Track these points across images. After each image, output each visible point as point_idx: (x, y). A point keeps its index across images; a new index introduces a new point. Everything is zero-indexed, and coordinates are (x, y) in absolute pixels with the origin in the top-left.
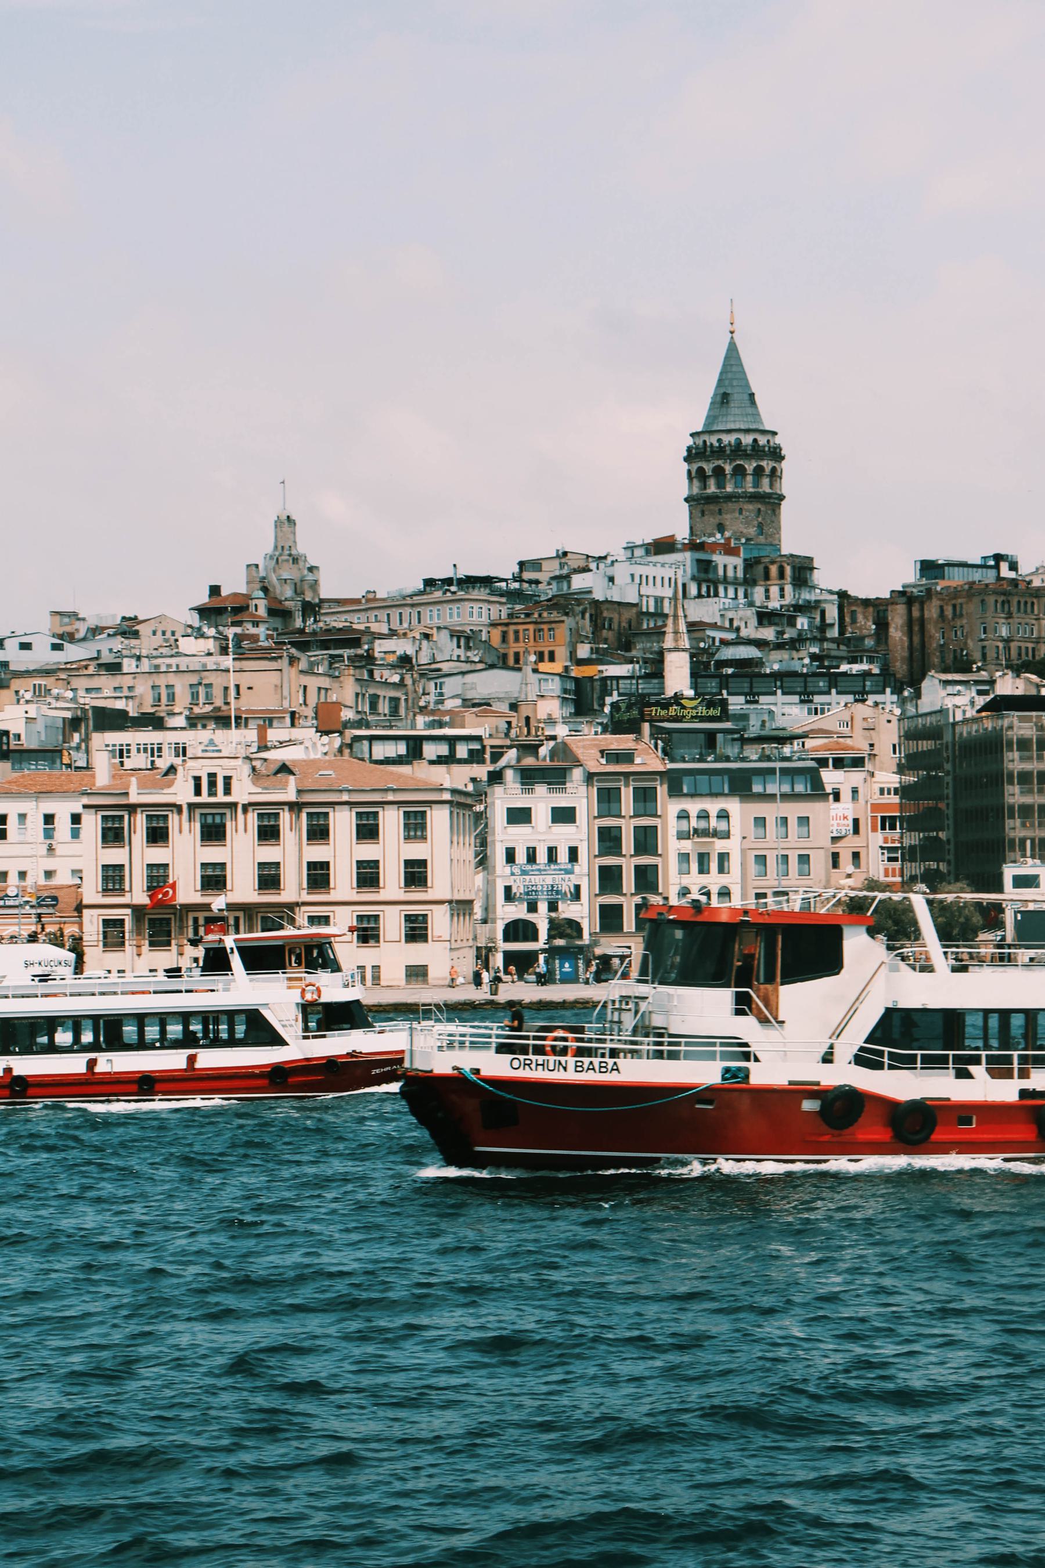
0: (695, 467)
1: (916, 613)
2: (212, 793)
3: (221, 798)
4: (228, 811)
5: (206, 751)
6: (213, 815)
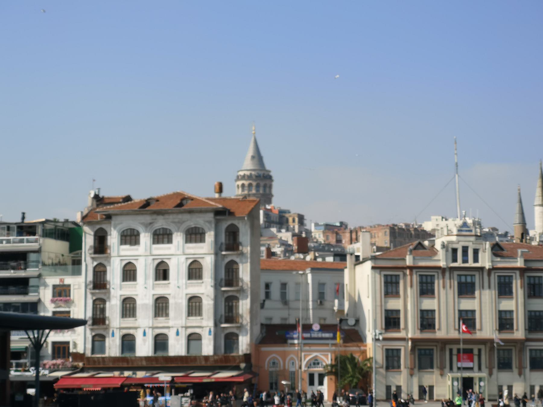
0: (240, 183)
2: (465, 261)
3: (471, 264)
4: (477, 274)
5: (461, 231)
6: (466, 276)
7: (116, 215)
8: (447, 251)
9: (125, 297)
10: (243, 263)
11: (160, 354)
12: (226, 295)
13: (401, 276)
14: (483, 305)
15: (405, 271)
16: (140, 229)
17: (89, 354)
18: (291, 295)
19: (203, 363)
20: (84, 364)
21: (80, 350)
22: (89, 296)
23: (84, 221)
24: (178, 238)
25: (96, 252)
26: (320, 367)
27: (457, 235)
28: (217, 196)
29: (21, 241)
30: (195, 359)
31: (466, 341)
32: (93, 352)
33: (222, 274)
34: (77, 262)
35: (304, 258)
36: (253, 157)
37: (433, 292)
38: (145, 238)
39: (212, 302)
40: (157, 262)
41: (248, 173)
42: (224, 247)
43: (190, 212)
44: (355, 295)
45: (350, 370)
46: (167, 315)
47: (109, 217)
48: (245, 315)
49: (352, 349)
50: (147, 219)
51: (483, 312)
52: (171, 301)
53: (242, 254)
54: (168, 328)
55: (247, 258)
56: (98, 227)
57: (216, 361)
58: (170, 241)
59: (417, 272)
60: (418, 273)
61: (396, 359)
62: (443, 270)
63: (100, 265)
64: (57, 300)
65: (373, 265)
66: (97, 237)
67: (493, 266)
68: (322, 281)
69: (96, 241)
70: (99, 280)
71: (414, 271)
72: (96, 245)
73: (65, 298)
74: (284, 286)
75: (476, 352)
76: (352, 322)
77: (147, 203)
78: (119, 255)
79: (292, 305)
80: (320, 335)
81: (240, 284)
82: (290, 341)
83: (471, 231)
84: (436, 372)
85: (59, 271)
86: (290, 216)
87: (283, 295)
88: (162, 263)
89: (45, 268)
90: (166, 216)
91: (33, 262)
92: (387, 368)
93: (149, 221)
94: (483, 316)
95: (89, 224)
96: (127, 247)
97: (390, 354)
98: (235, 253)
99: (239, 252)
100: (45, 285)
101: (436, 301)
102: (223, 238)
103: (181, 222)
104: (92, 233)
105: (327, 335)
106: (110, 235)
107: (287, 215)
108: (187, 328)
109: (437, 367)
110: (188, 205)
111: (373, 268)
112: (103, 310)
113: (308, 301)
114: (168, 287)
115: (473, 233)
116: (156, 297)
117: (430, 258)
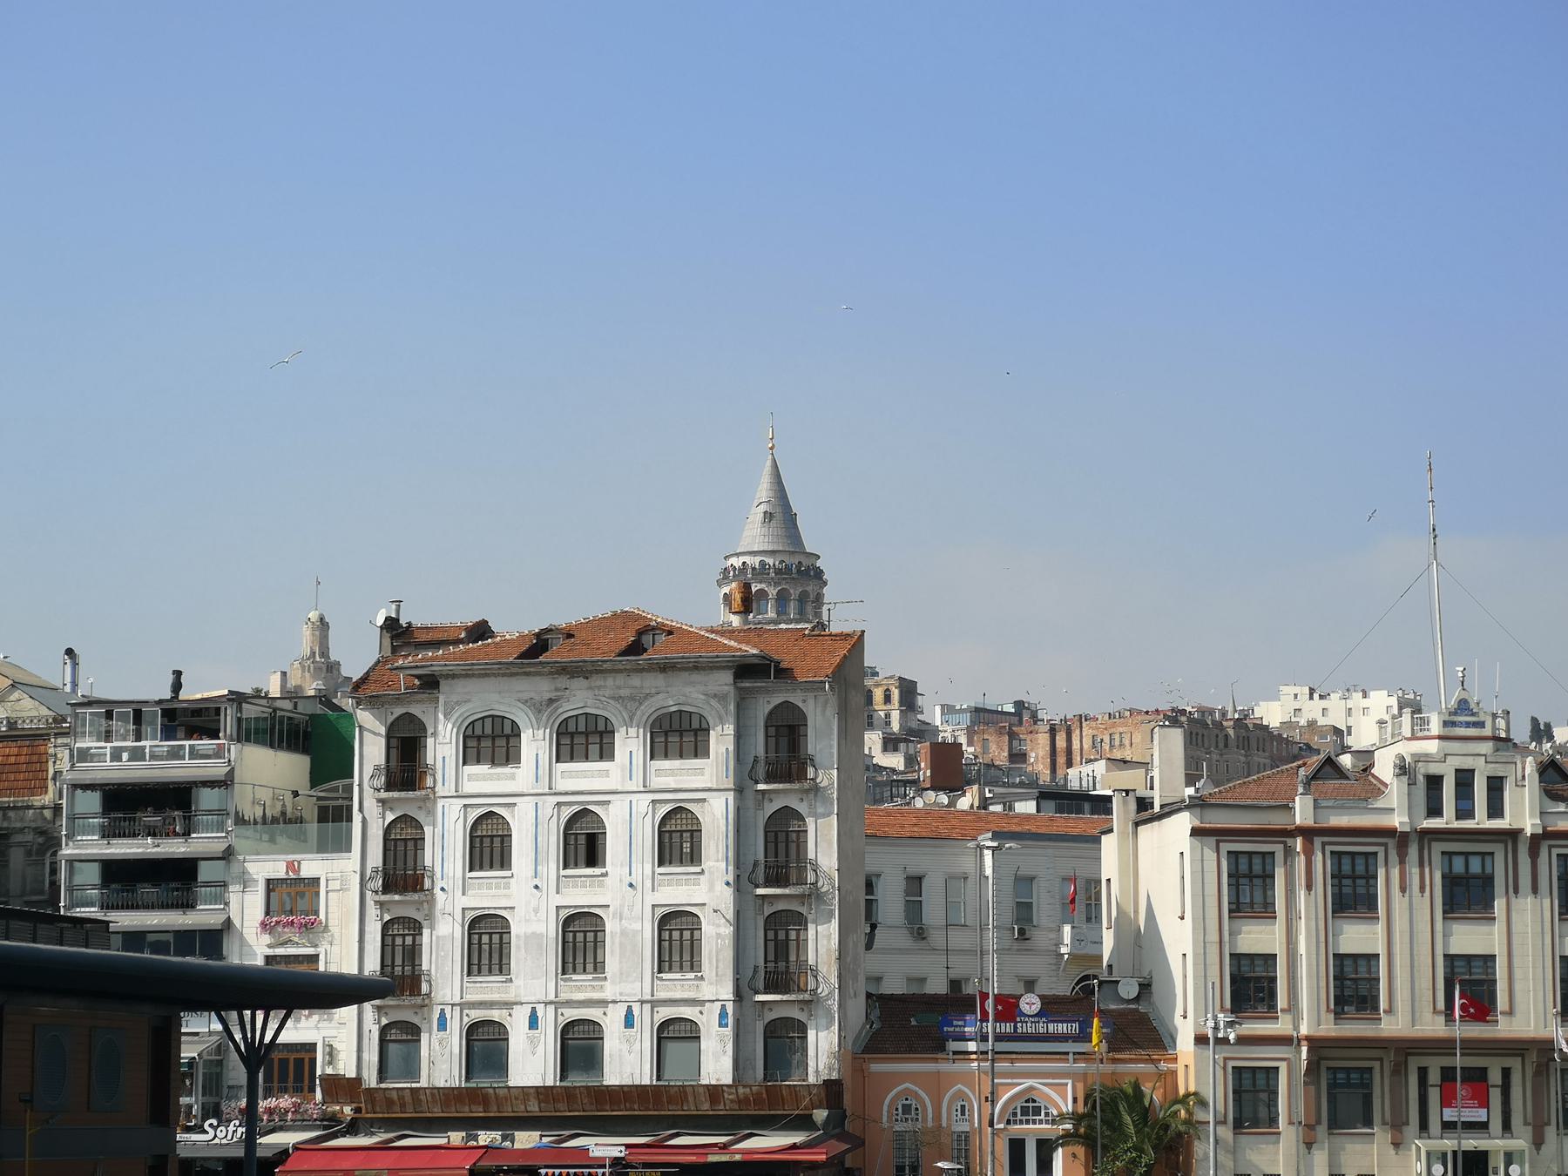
1: (1061, 742)
2: (1464, 812)
3: (1481, 820)
4: (1498, 851)
5: (1454, 724)
6: (1467, 854)
7: (454, 676)
8: (1412, 783)
9: (479, 913)
10: (816, 816)
11: (578, 1080)
12: (768, 910)
13: (1279, 857)
14: (1516, 940)
15: (1289, 841)
16: (521, 717)
17: (371, 1079)
18: (933, 913)
19: (705, 1108)
20: (358, 1110)
21: (346, 1067)
22: (372, 911)
23: (360, 694)
24: (630, 743)
25: (389, 786)
26: (1041, 1122)
27: (1440, 737)
28: (736, 621)
29: (175, 754)
30: (681, 1095)
31: (1471, 1047)
32: (382, 1073)
33: (758, 850)
34: (335, 815)
35: (952, 803)
36: (768, 516)
37: (1371, 904)
38: (535, 744)
39: (728, 931)
40: (567, 812)
41: (754, 561)
42: (761, 771)
43: (666, 667)
44: (1136, 912)
45: (1132, 1129)
46: (599, 967)
47: (430, 683)
48: (823, 969)
49: (1134, 1068)
50: (542, 687)
51: (1516, 961)
52: (610, 926)
53: (816, 789)
54: (603, 1003)
55: (827, 801)
56: (399, 711)
57: (742, 1102)
58: (606, 753)
59: (1324, 844)
60: (1329, 848)
61: (1264, 1096)
62: (1400, 839)
63: (404, 819)
64: (278, 923)
65: (1197, 823)
66: (394, 742)
67: (1544, 828)
68: (1024, 872)
69: (394, 752)
70: (400, 864)
71: (1318, 841)
72: (393, 763)
73: (303, 919)
74: (915, 883)
75: (1495, 1077)
76: (1129, 989)
77: (539, 645)
78: (460, 793)
79: (937, 938)
80: (1041, 1028)
81: (811, 878)
82: (953, 1046)
83: (1481, 725)
84: (1381, 1135)
85: (282, 840)
86: (877, 685)
87: (914, 910)
88: (585, 813)
89: (243, 830)
90: (597, 681)
91: (210, 812)
92: (1238, 1125)
93: (547, 696)
94: (1518, 974)
95: (374, 702)
96: (483, 769)
97: (1247, 1084)
98: (796, 786)
99: (806, 785)
100: (246, 882)
101: (1380, 927)
102: (758, 745)
103: (639, 699)
104: (383, 730)
105: (1063, 1028)
106: (434, 734)
107: (868, 682)
108: (654, 1004)
109: (1384, 1123)
110: (659, 649)
111: (1196, 832)
112: (413, 953)
113: (983, 928)
114: (601, 885)
115: (1487, 732)
116: (564, 914)
117: (1364, 804)
